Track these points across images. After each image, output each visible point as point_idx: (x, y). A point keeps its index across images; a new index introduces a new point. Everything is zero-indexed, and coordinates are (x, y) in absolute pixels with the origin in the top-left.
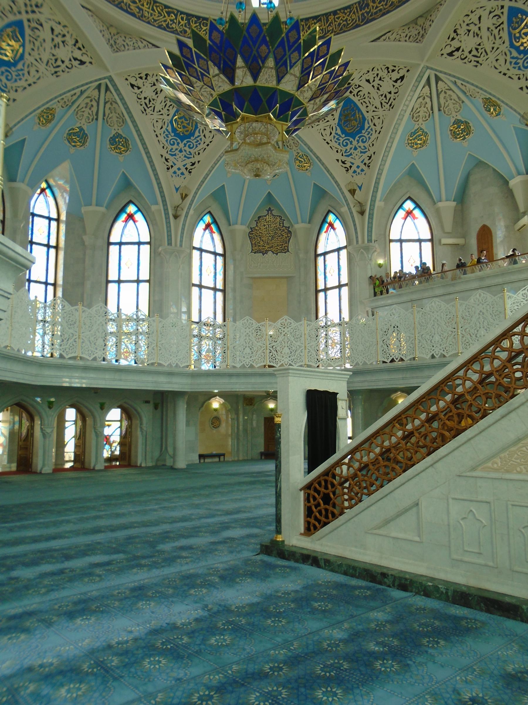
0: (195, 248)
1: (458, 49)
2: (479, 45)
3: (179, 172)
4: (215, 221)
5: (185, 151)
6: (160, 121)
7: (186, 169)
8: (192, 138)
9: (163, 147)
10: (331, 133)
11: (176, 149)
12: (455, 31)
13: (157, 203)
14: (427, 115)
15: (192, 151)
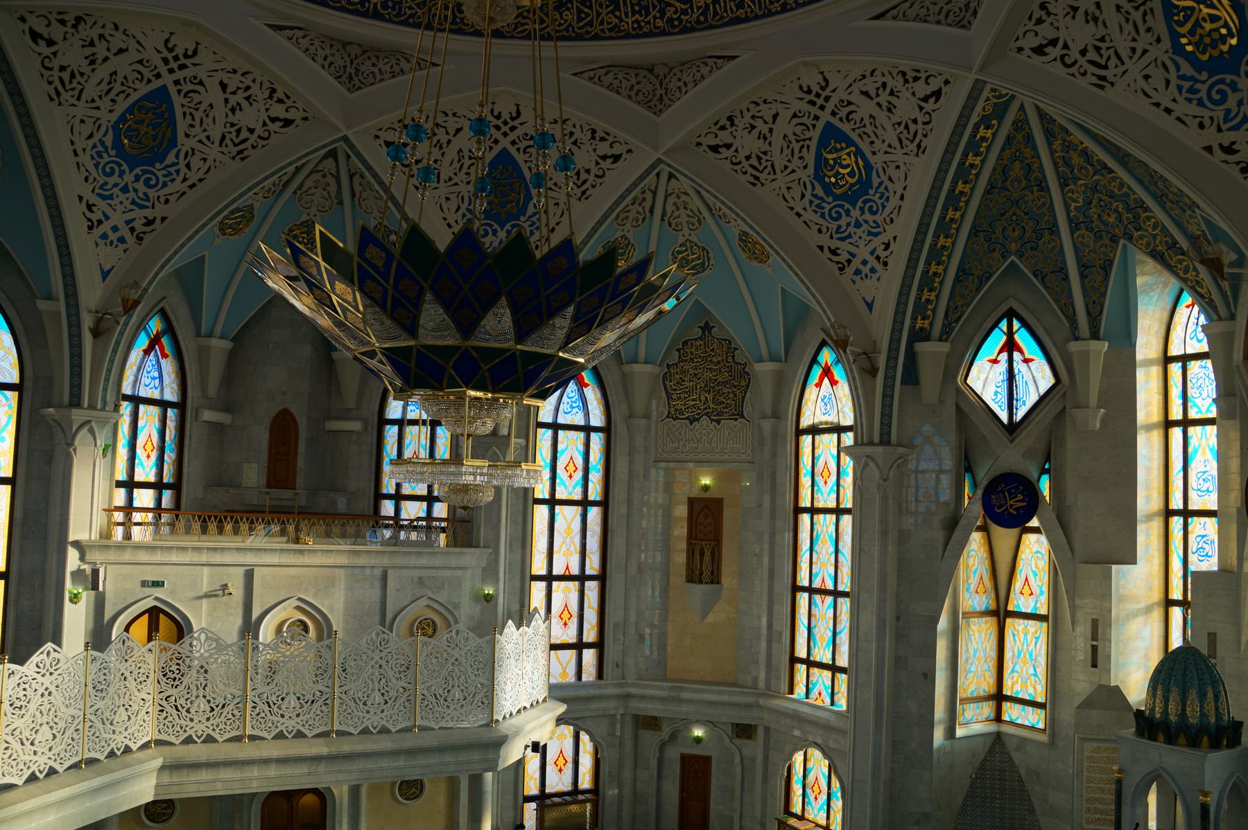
0: (126, 398)
1: (728, 146)
2: (765, 153)
3: (113, 237)
4: (169, 329)
5: (136, 191)
6: (89, 122)
7: (132, 230)
8: (158, 165)
9: (86, 179)
10: (459, 208)
11: (116, 185)
12: (730, 118)
13: (50, 297)
14: (641, 218)
15: (152, 193)
